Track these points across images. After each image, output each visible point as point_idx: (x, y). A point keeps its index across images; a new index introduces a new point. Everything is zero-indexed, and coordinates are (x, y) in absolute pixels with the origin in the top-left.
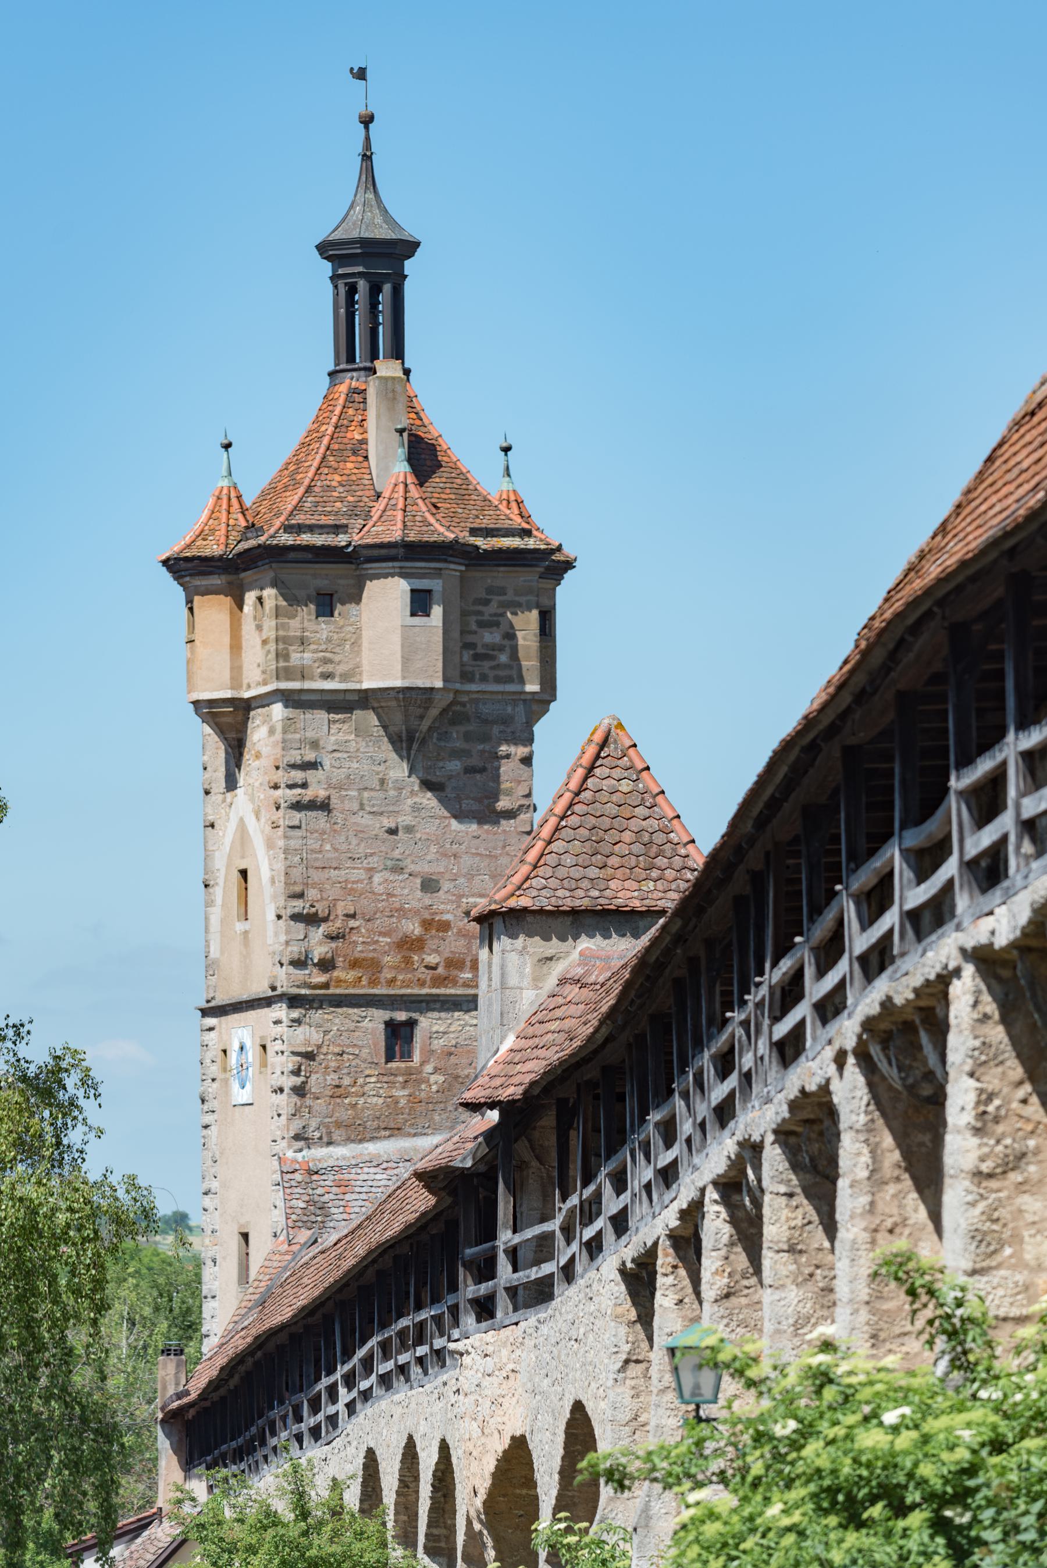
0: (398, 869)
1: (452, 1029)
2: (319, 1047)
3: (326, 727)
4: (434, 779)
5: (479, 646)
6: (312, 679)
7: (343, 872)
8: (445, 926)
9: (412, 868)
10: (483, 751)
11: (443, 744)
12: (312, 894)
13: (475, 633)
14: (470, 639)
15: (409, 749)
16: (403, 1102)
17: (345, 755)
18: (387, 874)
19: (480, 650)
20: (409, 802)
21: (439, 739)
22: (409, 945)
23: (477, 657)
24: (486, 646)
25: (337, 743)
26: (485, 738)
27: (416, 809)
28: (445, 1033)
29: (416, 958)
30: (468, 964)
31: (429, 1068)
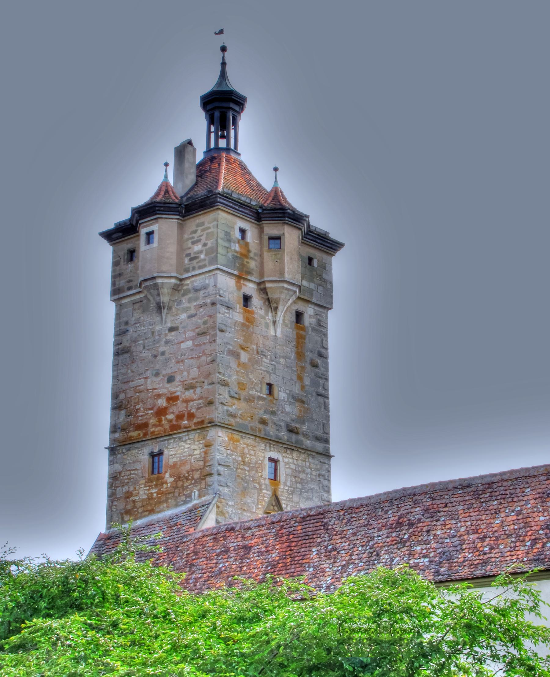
0: (157, 374)
1: (179, 452)
2: (120, 473)
3: (131, 314)
4: (174, 325)
5: (192, 254)
6: (123, 291)
7: (135, 382)
8: (176, 398)
9: (164, 372)
10: (195, 306)
11: (179, 307)
12: (122, 396)
13: (190, 248)
14: (188, 252)
15: (161, 313)
16: (155, 495)
17: (138, 325)
18: (154, 379)
19: (192, 256)
20: (164, 340)
21: (177, 305)
22: (161, 412)
23: (191, 259)
24: (195, 253)
25: (135, 320)
26: (196, 299)
27: (167, 342)
28: (175, 455)
29: (163, 418)
30: (186, 415)
31: (167, 475)
